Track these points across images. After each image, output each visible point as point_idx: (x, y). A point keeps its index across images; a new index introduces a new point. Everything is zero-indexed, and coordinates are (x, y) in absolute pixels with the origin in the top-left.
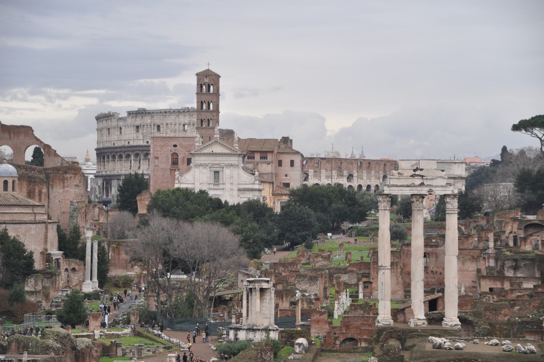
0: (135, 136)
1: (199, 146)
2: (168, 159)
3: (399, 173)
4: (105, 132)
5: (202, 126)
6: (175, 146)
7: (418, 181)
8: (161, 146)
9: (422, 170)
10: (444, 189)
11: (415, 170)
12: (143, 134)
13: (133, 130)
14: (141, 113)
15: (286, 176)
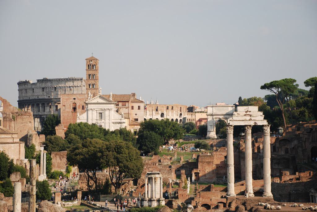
0: (42, 93)
1: (90, 99)
2: (71, 106)
3: (238, 114)
4: (24, 91)
5: (89, 88)
6: (74, 99)
7: (248, 118)
8: (66, 99)
9: (250, 112)
10: (263, 122)
11: (246, 112)
12: (46, 92)
13: (41, 90)
14: (45, 80)
15: (136, 115)
